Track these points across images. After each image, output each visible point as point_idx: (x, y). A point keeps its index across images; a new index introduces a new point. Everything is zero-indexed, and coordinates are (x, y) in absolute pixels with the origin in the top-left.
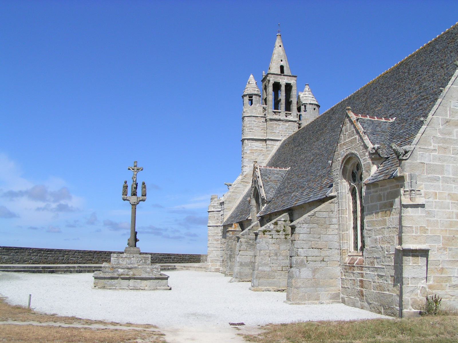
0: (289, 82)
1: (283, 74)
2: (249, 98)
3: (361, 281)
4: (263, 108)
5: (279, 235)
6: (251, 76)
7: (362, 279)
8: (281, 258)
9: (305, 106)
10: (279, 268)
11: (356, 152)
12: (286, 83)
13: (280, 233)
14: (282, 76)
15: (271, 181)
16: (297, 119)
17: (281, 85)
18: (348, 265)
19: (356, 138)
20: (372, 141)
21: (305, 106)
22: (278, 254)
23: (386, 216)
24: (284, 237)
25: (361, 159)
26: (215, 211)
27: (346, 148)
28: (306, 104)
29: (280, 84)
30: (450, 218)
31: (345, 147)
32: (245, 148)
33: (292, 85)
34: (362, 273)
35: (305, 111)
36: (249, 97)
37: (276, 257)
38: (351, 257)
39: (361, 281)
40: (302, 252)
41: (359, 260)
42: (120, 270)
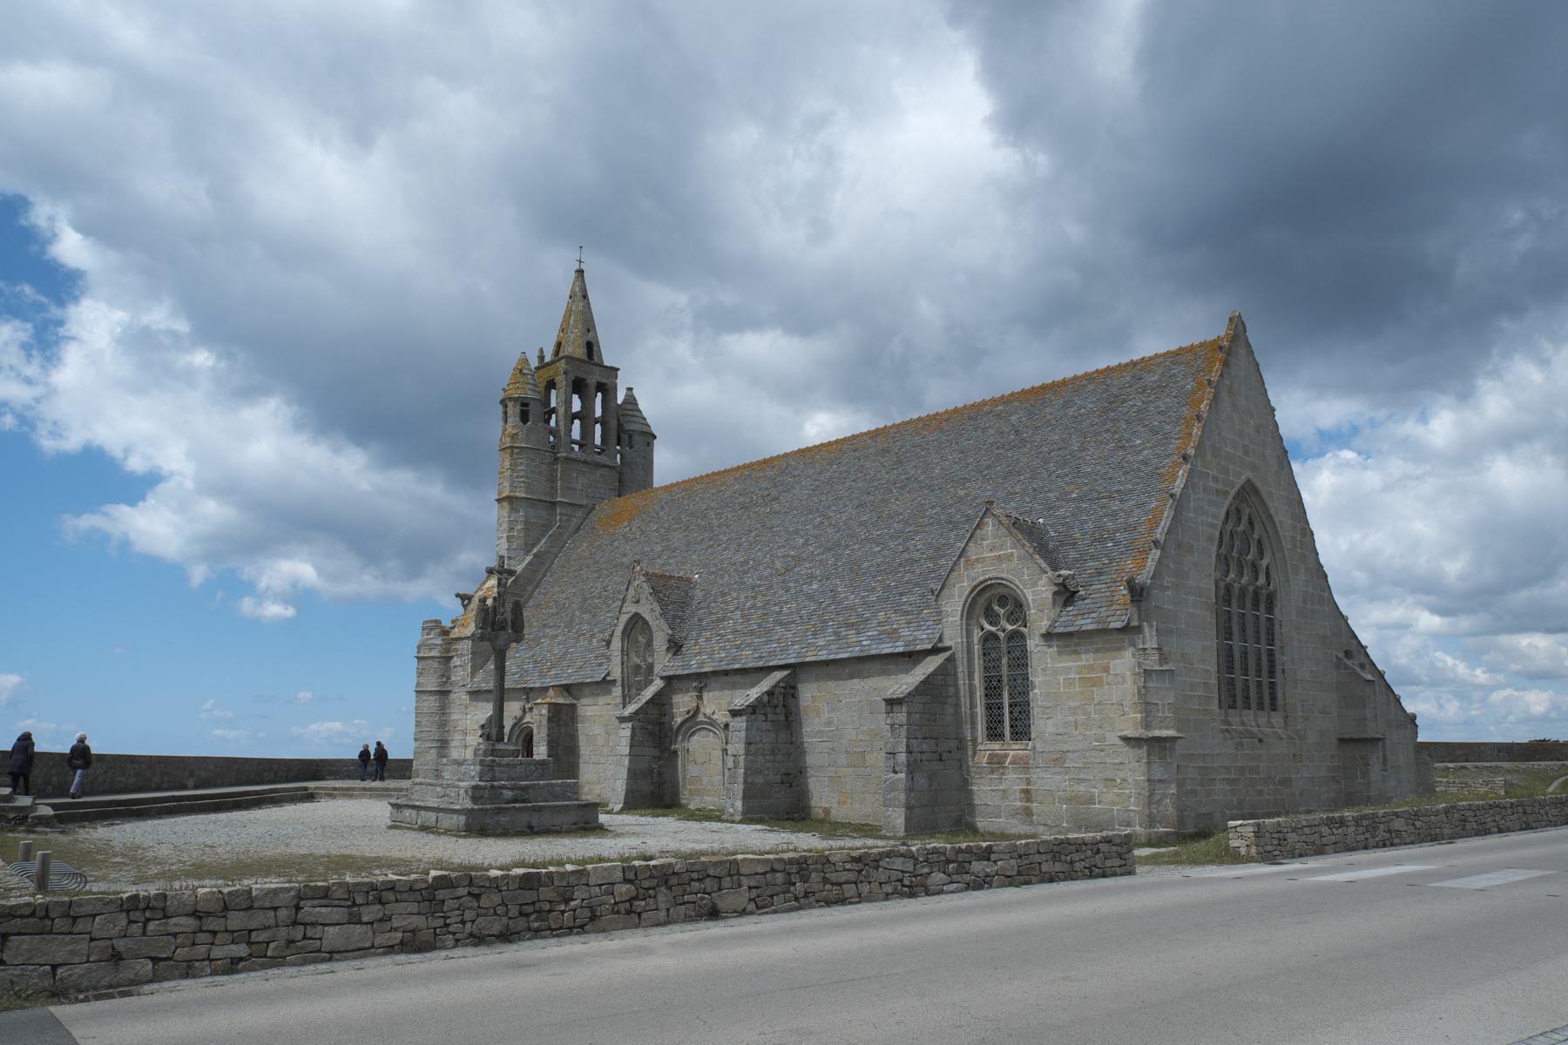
0: (604, 381)
3: (1027, 792)
5: (776, 714)
7: (1029, 787)
8: (779, 758)
10: (779, 779)
11: (1010, 577)
13: (778, 710)
15: (671, 603)
17: (587, 384)
18: (985, 765)
19: (1012, 555)
21: (630, 436)
22: (776, 751)
23: (1093, 686)
24: (782, 718)
25: (1025, 591)
27: (982, 567)
30: (1183, 691)
31: (980, 566)
34: (1028, 778)
37: (772, 757)
38: (988, 752)
39: (1027, 792)
40: (915, 745)
41: (1013, 756)
42: (504, 791)
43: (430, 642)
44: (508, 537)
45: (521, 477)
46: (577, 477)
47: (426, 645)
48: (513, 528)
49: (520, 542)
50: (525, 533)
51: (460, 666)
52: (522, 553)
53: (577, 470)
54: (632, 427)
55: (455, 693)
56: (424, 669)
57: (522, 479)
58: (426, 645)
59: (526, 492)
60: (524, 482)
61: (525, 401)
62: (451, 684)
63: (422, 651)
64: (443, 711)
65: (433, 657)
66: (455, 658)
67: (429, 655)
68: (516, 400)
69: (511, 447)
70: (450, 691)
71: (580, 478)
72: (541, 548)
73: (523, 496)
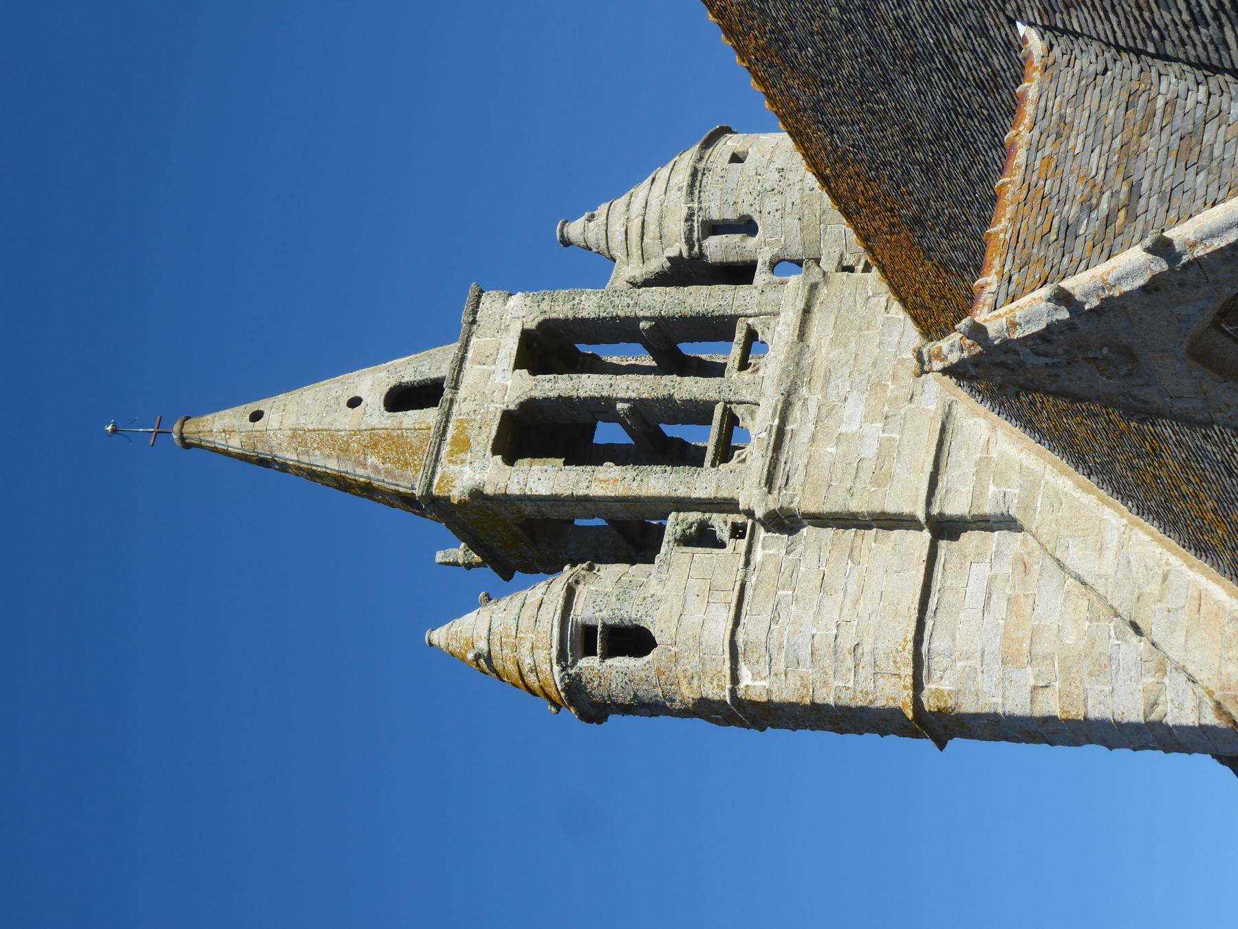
1: (447, 394)
2: (593, 653)
4: (686, 540)
6: (439, 636)
9: (714, 228)
12: (518, 365)
14: (462, 392)
16: (795, 282)
20: (1199, 202)
28: (689, 218)
29: (512, 407)
32: (1000, 701)
33: (532, 325)
35: (747, 226)
36: (589, 651)
53: (813, 439)
54: (676, 227)
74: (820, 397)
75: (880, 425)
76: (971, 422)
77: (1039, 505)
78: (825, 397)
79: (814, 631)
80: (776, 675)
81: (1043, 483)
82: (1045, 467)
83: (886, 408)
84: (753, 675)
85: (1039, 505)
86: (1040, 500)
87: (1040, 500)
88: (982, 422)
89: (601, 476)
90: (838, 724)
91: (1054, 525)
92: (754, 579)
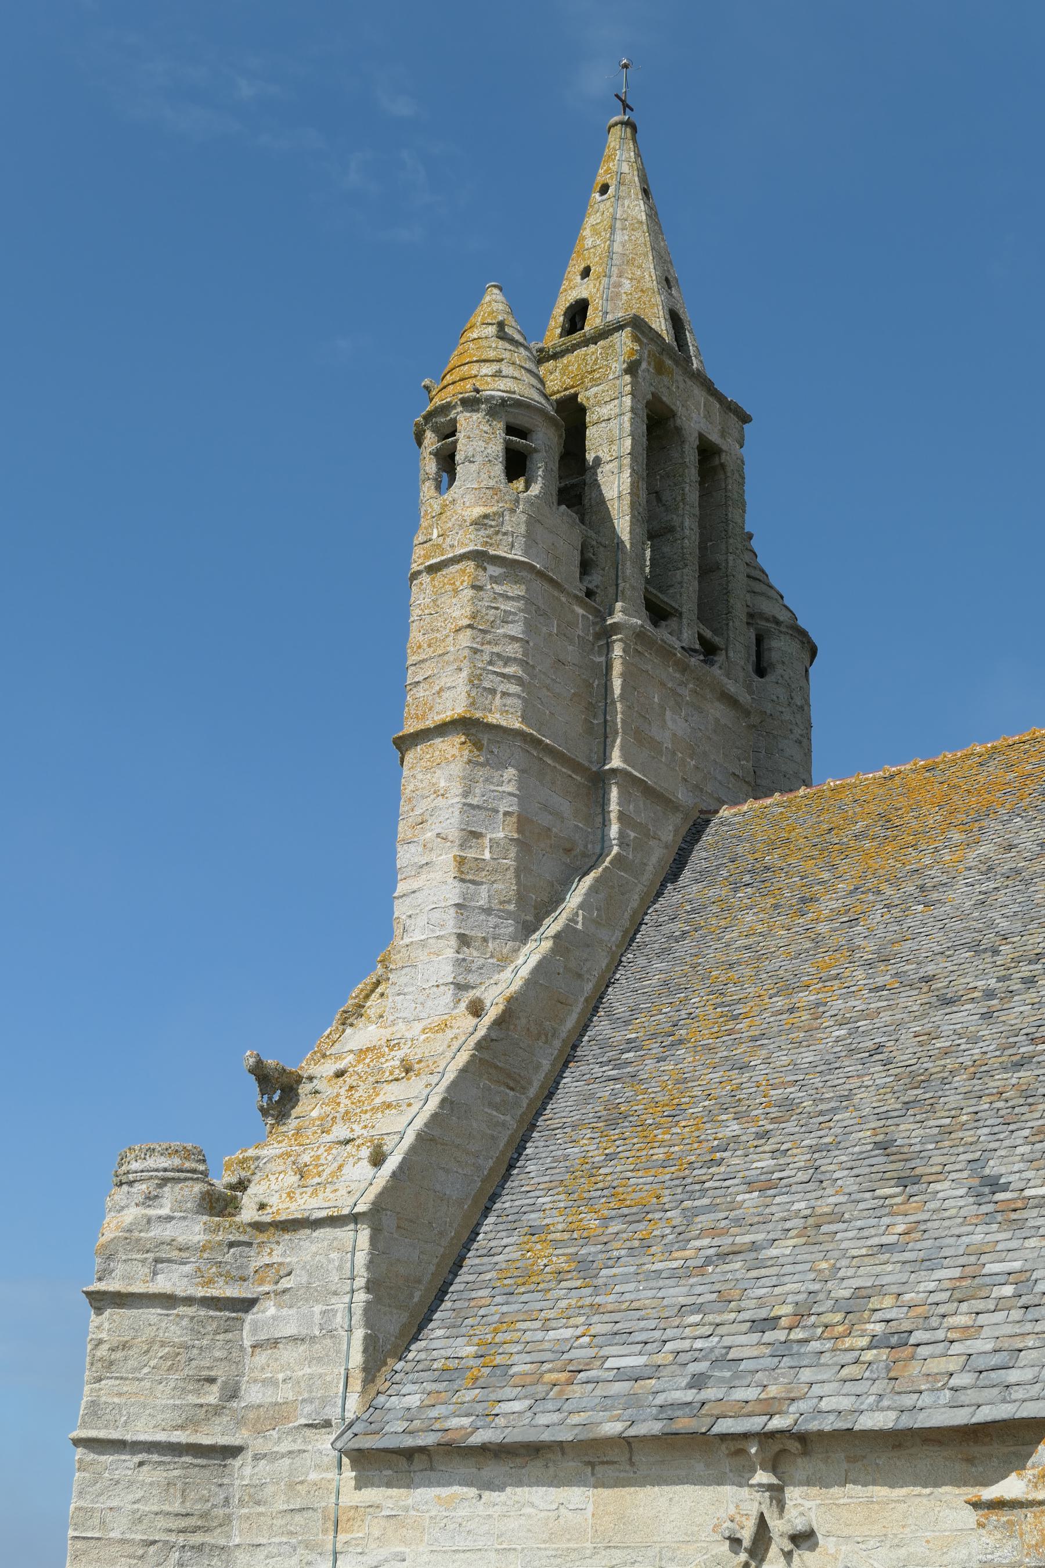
26: (189, 1301)
43: (156, 1232)
44: (461, 861)
45: (507, 661)
46: (663, 708)
47: (138, 1245)
48: (477, 835)
49: (505, 886)
50: (517, 859)
51: (295, 1339)
52: (509, 927)
55: (256, 1458)
56: (125, 1346)
57: (510, 670)
58: (138, 1245)
59: (524, 719)
60: (519, 681)
61: (522, 420)
62: (240, 1422)
63: (120, 1269)
64: (197, 1539)
65: (168, 1300)
66: (269, 1309)
67: (153, 1288)
68: (499, 408)
69: (480, 558)
70: (233, 1451)
71: (668, 713)
72: (572, 920)
73: (517, 725)
74: (688, 698)
75: (670, 746)
76: (671, 828)
77: (622, 874)
78: (687, 703)
79: (531, 644)
80: (495, 598)
81: (636, 881)
82: (645, 886)
83: (680, 755)
84: (496, 577)
85: (622, 874)
86: (625, 876)
87: (625, 876)
88: (671, 838)
89: (640, 483)
90: (429, 646)
91: (611, 884)
92: (564, 599)
